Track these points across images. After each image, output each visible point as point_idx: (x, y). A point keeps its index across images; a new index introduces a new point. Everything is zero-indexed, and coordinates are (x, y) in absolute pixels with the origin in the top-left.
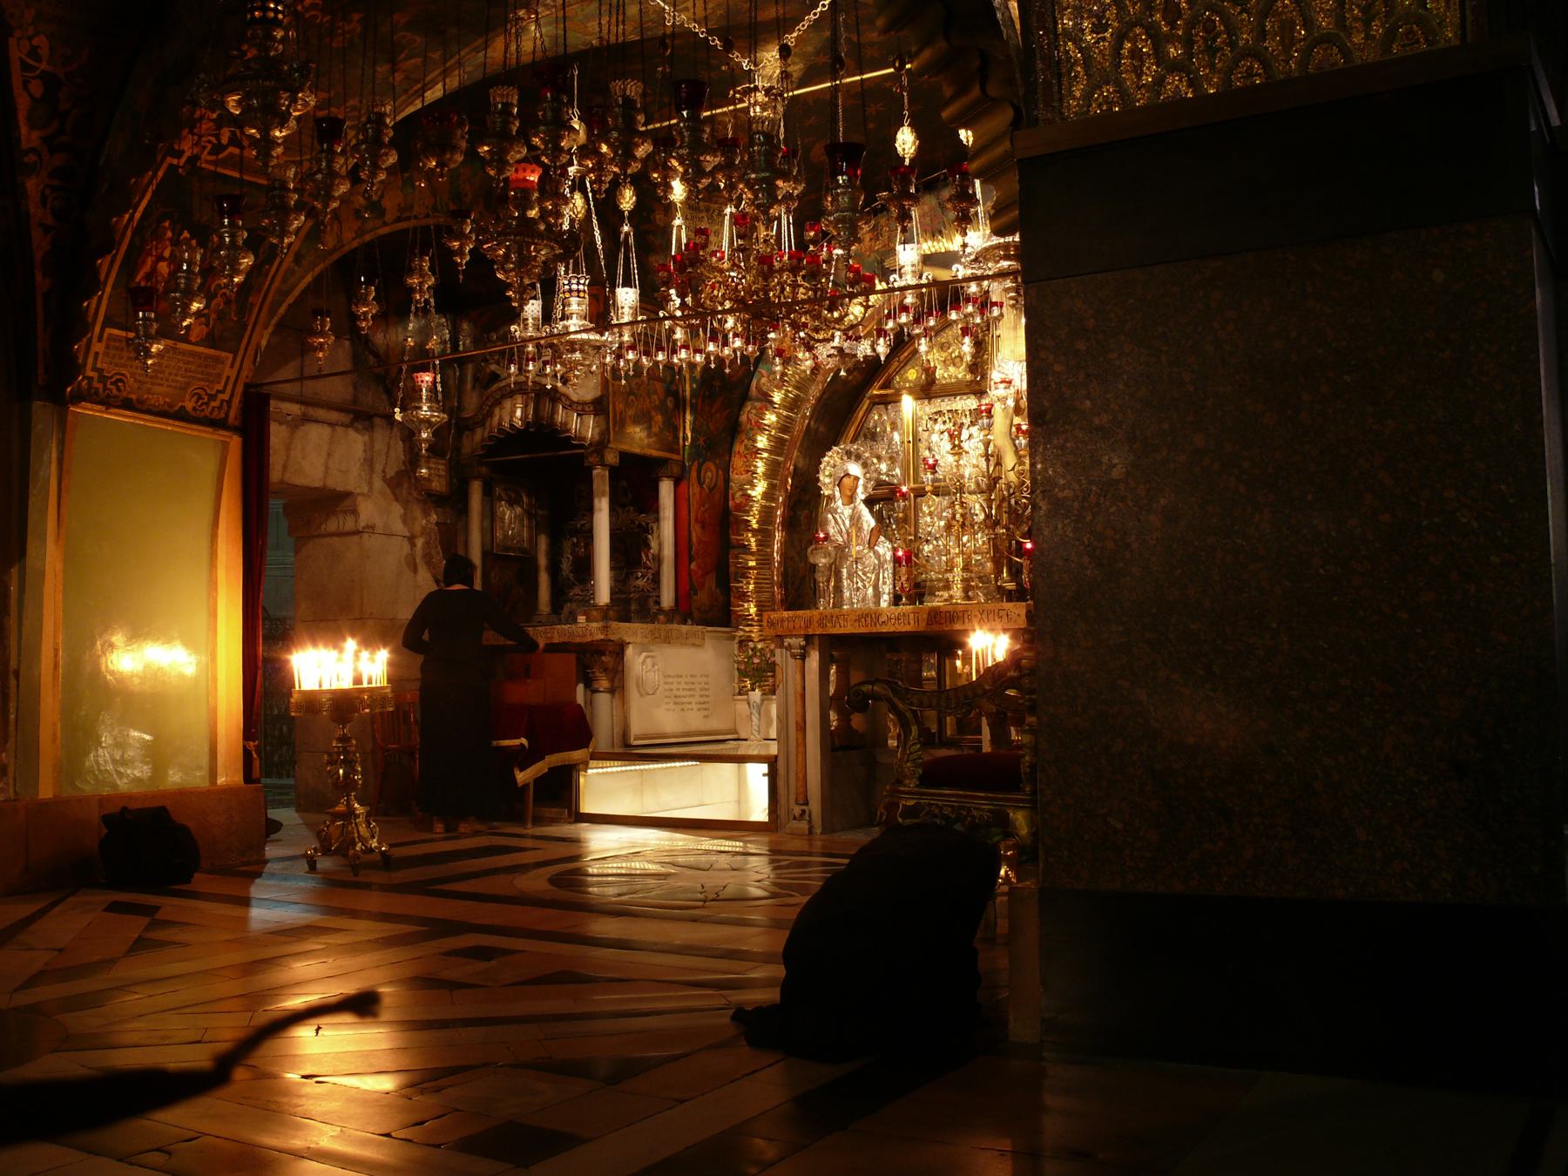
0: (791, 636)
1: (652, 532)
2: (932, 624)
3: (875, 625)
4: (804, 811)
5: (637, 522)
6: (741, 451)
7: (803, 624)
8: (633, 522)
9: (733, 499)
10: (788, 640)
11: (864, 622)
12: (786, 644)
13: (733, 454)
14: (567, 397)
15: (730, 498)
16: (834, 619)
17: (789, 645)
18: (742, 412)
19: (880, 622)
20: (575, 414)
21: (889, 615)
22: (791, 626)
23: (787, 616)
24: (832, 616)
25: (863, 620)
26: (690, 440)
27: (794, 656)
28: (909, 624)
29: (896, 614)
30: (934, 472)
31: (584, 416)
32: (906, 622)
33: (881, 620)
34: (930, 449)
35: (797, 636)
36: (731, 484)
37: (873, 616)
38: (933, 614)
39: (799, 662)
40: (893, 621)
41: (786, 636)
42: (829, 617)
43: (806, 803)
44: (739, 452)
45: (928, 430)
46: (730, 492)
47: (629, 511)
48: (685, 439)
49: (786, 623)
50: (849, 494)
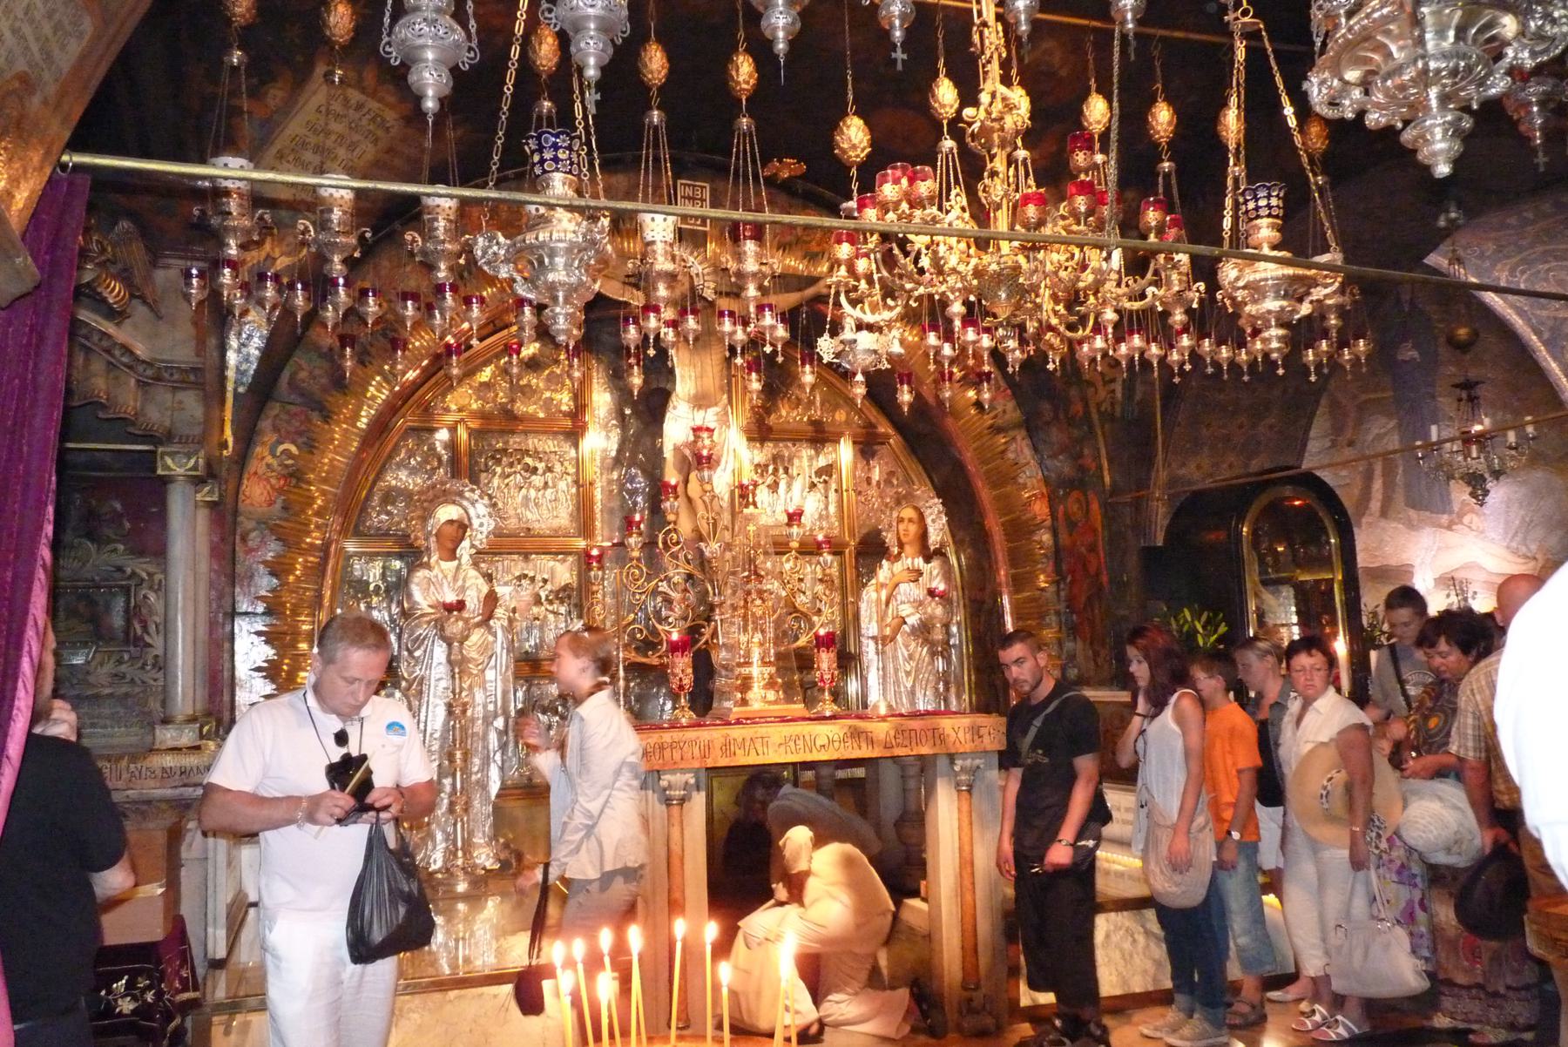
0: (673, 772)
1: (159, 589)
5: (129, 570)
6: (260, 472)
7: (696, 751)
8: (120, 569)
10: (668, 777)
12: (664, 783)
13: (246, 476)
14: (127, 350)
16: (747, 744)
22: (677, 756)
23: (669, 740)
25: (792, 744)
26: (230, 449)
27: (668, 801)
33: (819, 743)
35: (683, 771)
37: (807, 738)
39: (675, 810)
40: (836, 744)
41: (666, 773)
42: (740, 740)
44: (256, 473)
47: (115, 550)
48: (224, 445)
49: (667, 753)
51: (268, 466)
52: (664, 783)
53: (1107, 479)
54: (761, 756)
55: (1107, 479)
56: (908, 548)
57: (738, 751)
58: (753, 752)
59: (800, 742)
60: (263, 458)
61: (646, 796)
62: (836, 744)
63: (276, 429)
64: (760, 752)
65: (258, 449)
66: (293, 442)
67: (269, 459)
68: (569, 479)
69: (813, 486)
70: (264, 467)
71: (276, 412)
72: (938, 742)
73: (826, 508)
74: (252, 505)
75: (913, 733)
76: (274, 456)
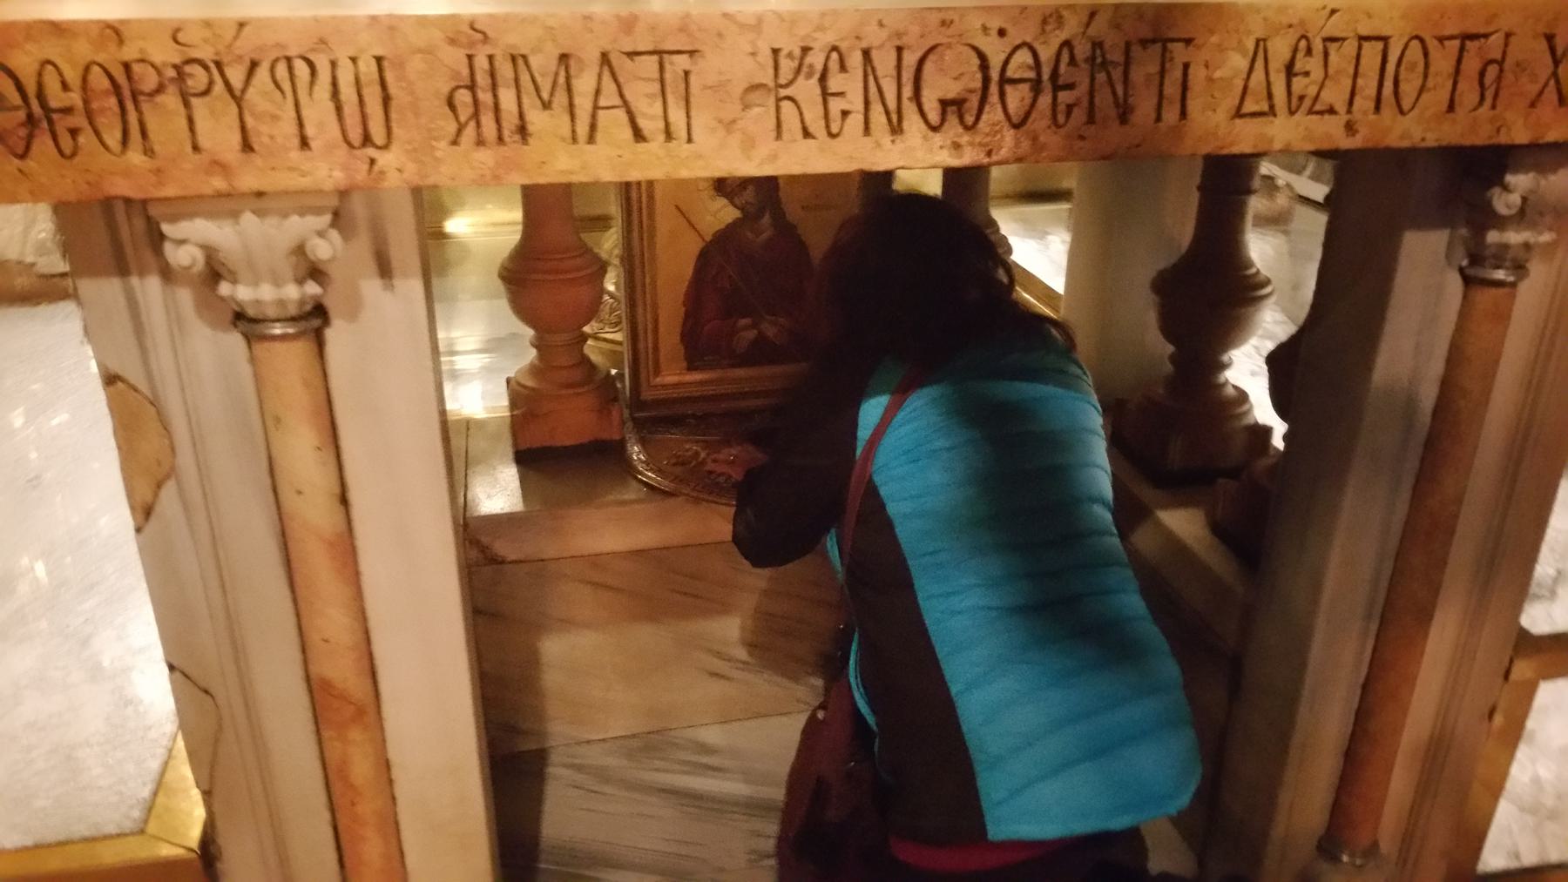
0: (226, 204)
3: (896, 129)
16: (584, 84)
17: (210, 253)
24: (564, 58)
25: (807, 89)
29: (1046, 54)
32: (1104, 100)
42: (542, 63)
57: (537, 119)
58: (614, 123)
59: (849, 85)
72: (1468, 93)
75: (1372, 51)
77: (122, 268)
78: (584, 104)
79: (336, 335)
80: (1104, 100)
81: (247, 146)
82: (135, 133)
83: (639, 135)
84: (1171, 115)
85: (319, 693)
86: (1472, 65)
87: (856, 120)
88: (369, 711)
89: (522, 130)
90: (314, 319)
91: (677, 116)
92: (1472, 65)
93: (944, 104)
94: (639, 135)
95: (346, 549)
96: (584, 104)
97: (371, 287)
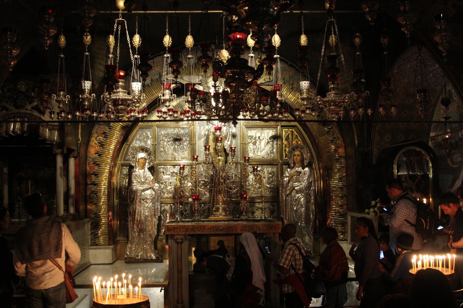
0: (178, 235)
2: (243, 231)
3: (218, 231)
4: (182, 306)
6: (93, 145)
7: (184, 230)
9: (89, 164)
11: (213, 230)
15: (87, 164)
16: (199, 228)
17: (177, 238)
18: (93, 129)
19: (220, 230)
20: (48, 130)
21: (224, 227)
24: (198, 227)
25: (212, 229)
26: (80, 141)
28: (233, 231)
30: (197, 161)
31: (52, 131)
34: (164, 148)
36: (88, 158)
37: (217, 227)
38: (243, 227)
39: (180, 245)
40: (226, 229)
41: (176, 235)
42: (197, 227)
43: (182, 303)
44: (92, 145)
45: (163, 140)
46: (87, 162)
49: (176, 230)
50: (142, 165)
51: (95, 143)
52: (175, 238)
53: (356, 142)
54: (203, 232)
55: (356, 142)
56: (297, 165)
57: (196, 230)
60: (94, 141)
61: (171, 242)
62: (226, 229)
63: (97, 133)
64: (203, 231)
65: (92, 139)
66: (102, 136)
67: (95, 141)
68: (188, 142)
69: (268, 142)
70: (94, 144)
71: (97, 128)
73: (273, 150)
74: (91, 154)
75: (250, 227)
76: (97, 140)
77: (171, 239)
78: (199, 229)
79: (183, 245)
80: (231, 230)
81: (180, 232)
82: (174, 231)
83: (202, 231)
84: (236, 231)
85: (178, 270)
86: (257, 228)
87: (215, 231)
88: (181, 272)
89: (195, 231)
90: (181, 243)
91: (204, 230)
92: (257, 228)
93: (221, 230)
94: (202, 231)
95: (181, 259)
96: (199, 229)
97: (185, 241)
